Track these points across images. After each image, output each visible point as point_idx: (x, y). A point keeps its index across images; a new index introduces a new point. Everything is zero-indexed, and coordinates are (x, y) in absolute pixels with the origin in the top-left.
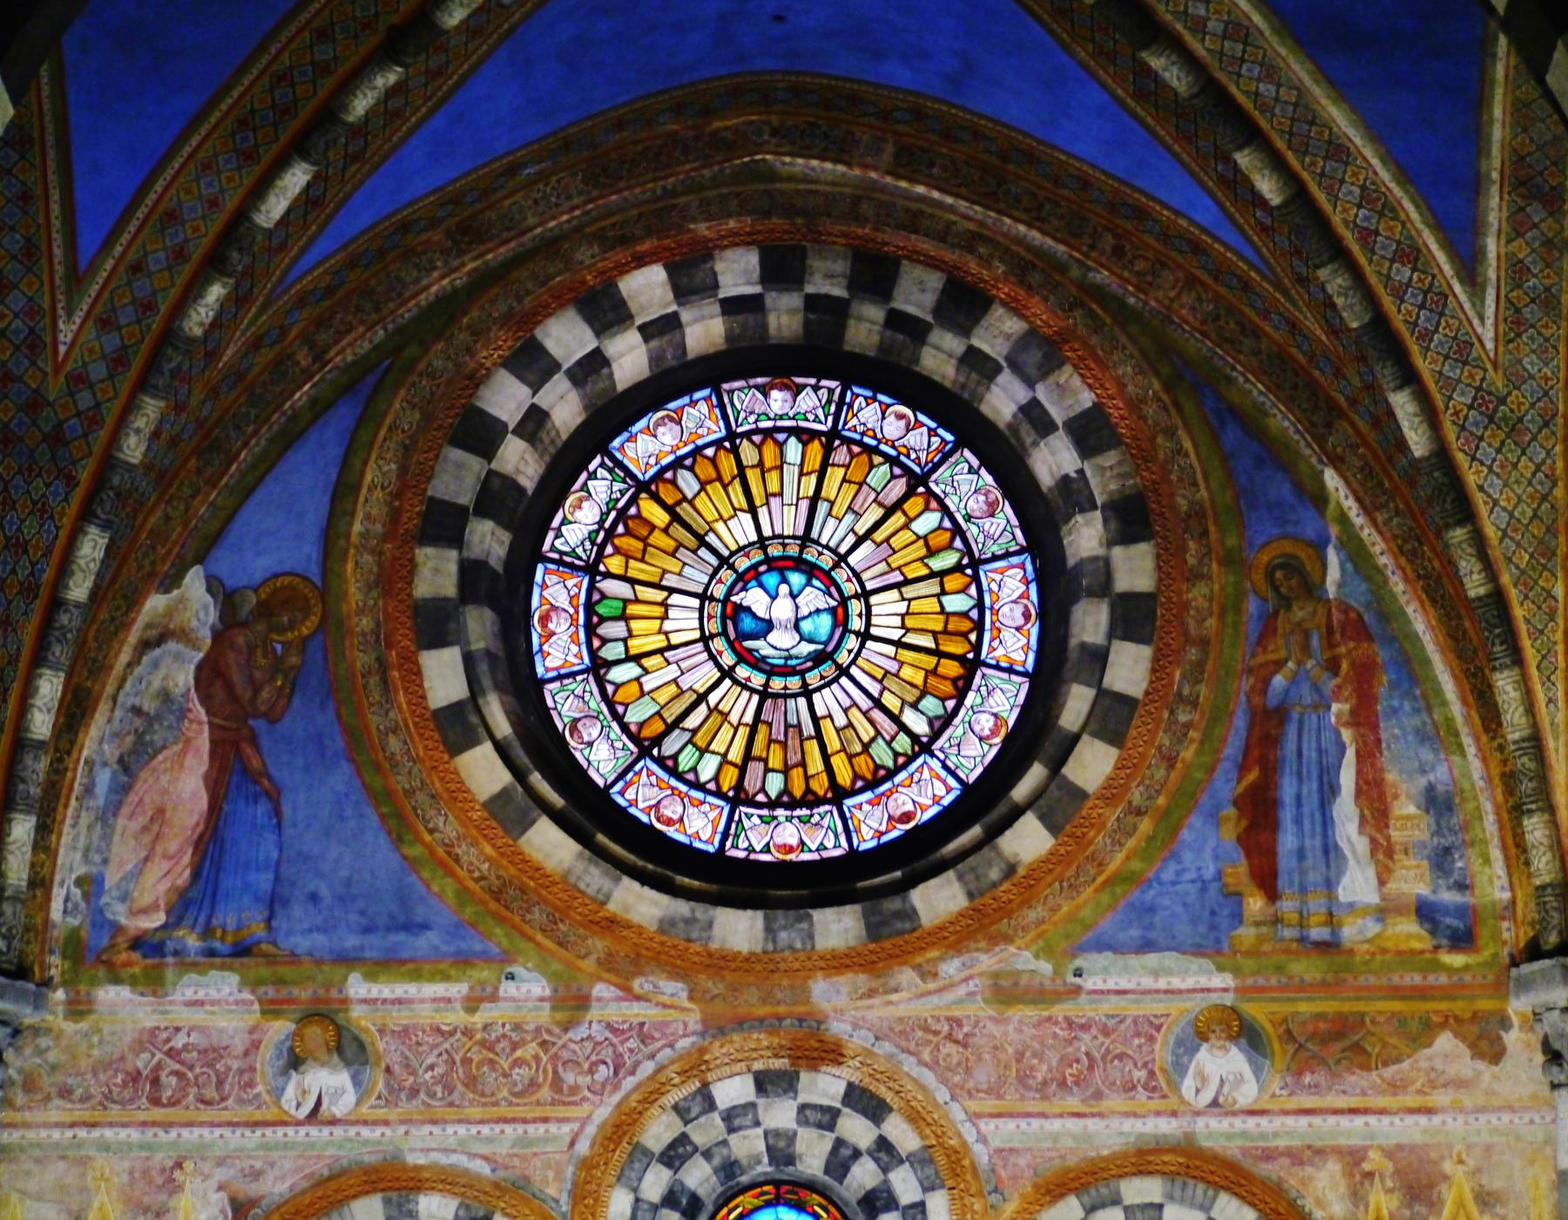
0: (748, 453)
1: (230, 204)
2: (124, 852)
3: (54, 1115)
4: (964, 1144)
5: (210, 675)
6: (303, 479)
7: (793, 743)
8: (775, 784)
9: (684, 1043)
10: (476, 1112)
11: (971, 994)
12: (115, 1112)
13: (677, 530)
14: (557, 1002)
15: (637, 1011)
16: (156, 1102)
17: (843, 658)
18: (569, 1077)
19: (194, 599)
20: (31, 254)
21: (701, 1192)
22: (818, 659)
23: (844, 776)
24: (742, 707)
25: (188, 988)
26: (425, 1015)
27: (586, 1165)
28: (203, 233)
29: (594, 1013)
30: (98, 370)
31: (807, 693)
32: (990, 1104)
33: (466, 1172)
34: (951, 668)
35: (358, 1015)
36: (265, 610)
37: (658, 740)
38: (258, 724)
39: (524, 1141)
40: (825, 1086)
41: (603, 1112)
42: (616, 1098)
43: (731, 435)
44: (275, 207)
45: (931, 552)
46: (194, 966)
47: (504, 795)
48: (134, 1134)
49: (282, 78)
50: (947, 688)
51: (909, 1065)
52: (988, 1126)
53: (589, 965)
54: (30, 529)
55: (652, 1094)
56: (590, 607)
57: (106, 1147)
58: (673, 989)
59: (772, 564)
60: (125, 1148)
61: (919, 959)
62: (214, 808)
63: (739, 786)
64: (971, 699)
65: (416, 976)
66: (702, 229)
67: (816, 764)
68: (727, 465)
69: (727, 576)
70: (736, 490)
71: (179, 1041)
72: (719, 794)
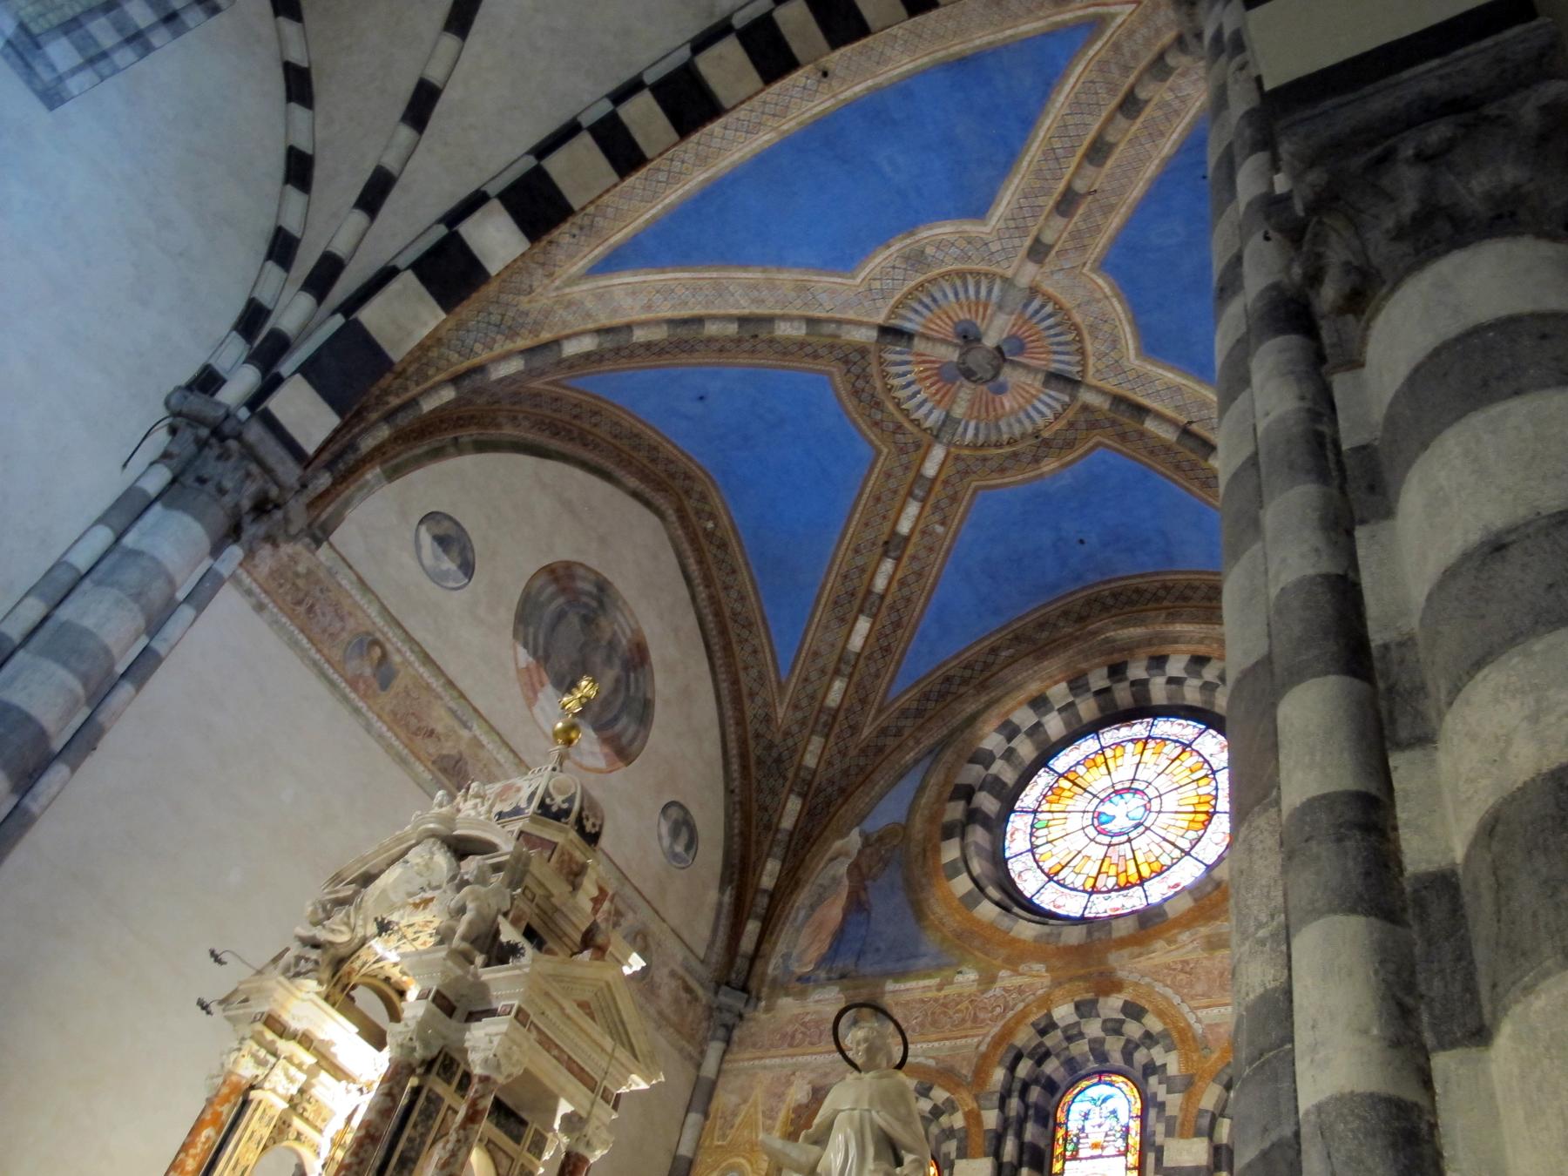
0: (1109, 753)
1: (840, 644)
2: (803, 941)
3: (747, 1055)
4: (1189, 1025)
5: (855, 867)
6: (908, 786)
7: (1122, 863)
8: (1111, 882)
9: (1040, 992)
10: (934, 1036)
11: (1195, 949)
12: (773, 1052)
13: (1076, 789)
14: (980, 982)
15: (1018, 981)
16: (791, 1045)
17: (1147, 824)
18: (982, 1015)
19: (854, 839)
20: (761, 678)
21: (1056, 1077)
22: (1136, 826)
23: (1145, 872)
24: (1097, 852)
25: (816, 996)
26: (917, 995)
27: (984, 1057)
28: (830, 661)
29: (999, 984)
30: (795, 728)
31: (1129, 840)
32: (1205, 1001)
33: (924, 1066)
34: (1202, 817)
35: (888, 1001)
36: (880, 839)
37: (1057, 874)
38: (869, 883)
39: (952, 1048)
40: (1112, 1005)
41: (995, 1030)
42: (1002, 1023)
43: (1102, 748)
44: (856, 642)
45: (1192, 772)
46: (823, 986)
47: (970, 893)
48: (777, 1061)
49: (846, 577)
50: (1200, 826)
51: (1159, 988)
52: (1202, 1013)
53: (998, 962)
54: (768, 800)
55: (1021, 1018)
56: (1032, 826)
57: (765, 1068)
58: (1039, 967)
59: (1116, 792)
60: (771, 1068)
61: (1168, 935)
62: (844, 918)
63: (1094, 886)
64: (1210, 828)
65: (918, 977)
66: (1084, 666)
67: (1132, 870)
68: (1100, 759)
69: (1096, 801)
70: (1103, 768)
71: (807, 1019)
72: (1084, 891)
